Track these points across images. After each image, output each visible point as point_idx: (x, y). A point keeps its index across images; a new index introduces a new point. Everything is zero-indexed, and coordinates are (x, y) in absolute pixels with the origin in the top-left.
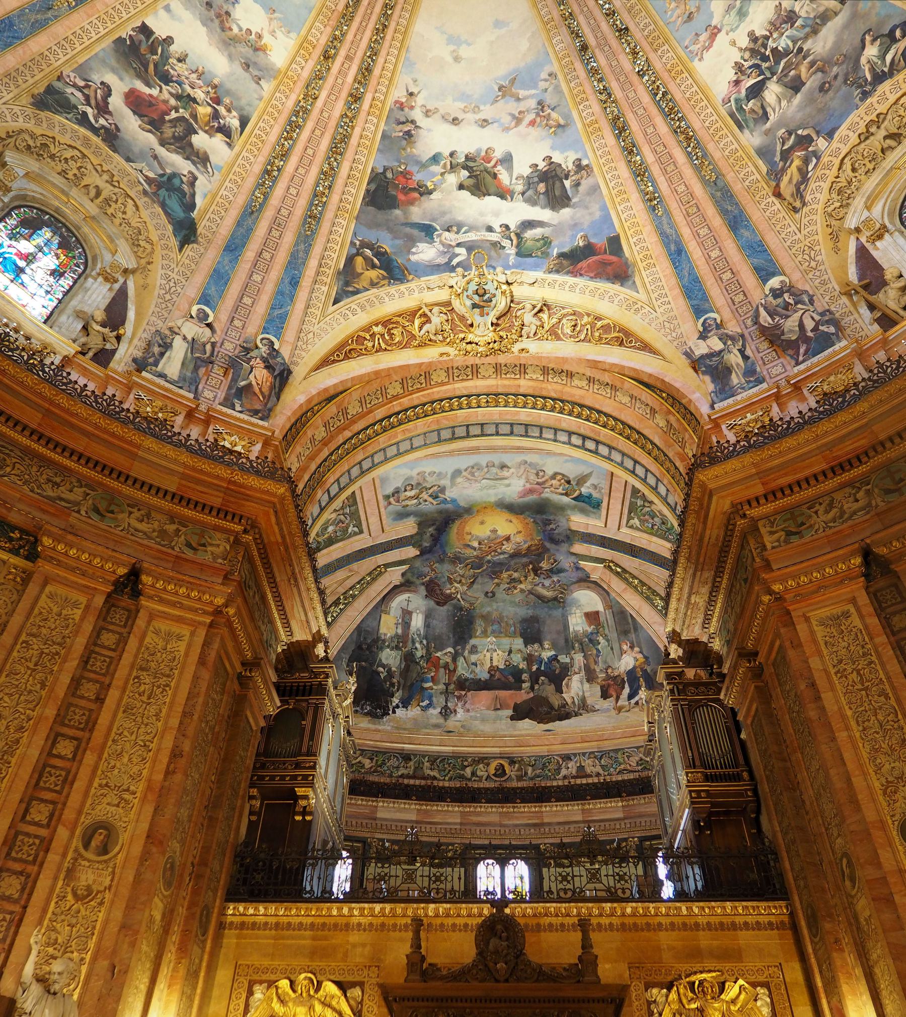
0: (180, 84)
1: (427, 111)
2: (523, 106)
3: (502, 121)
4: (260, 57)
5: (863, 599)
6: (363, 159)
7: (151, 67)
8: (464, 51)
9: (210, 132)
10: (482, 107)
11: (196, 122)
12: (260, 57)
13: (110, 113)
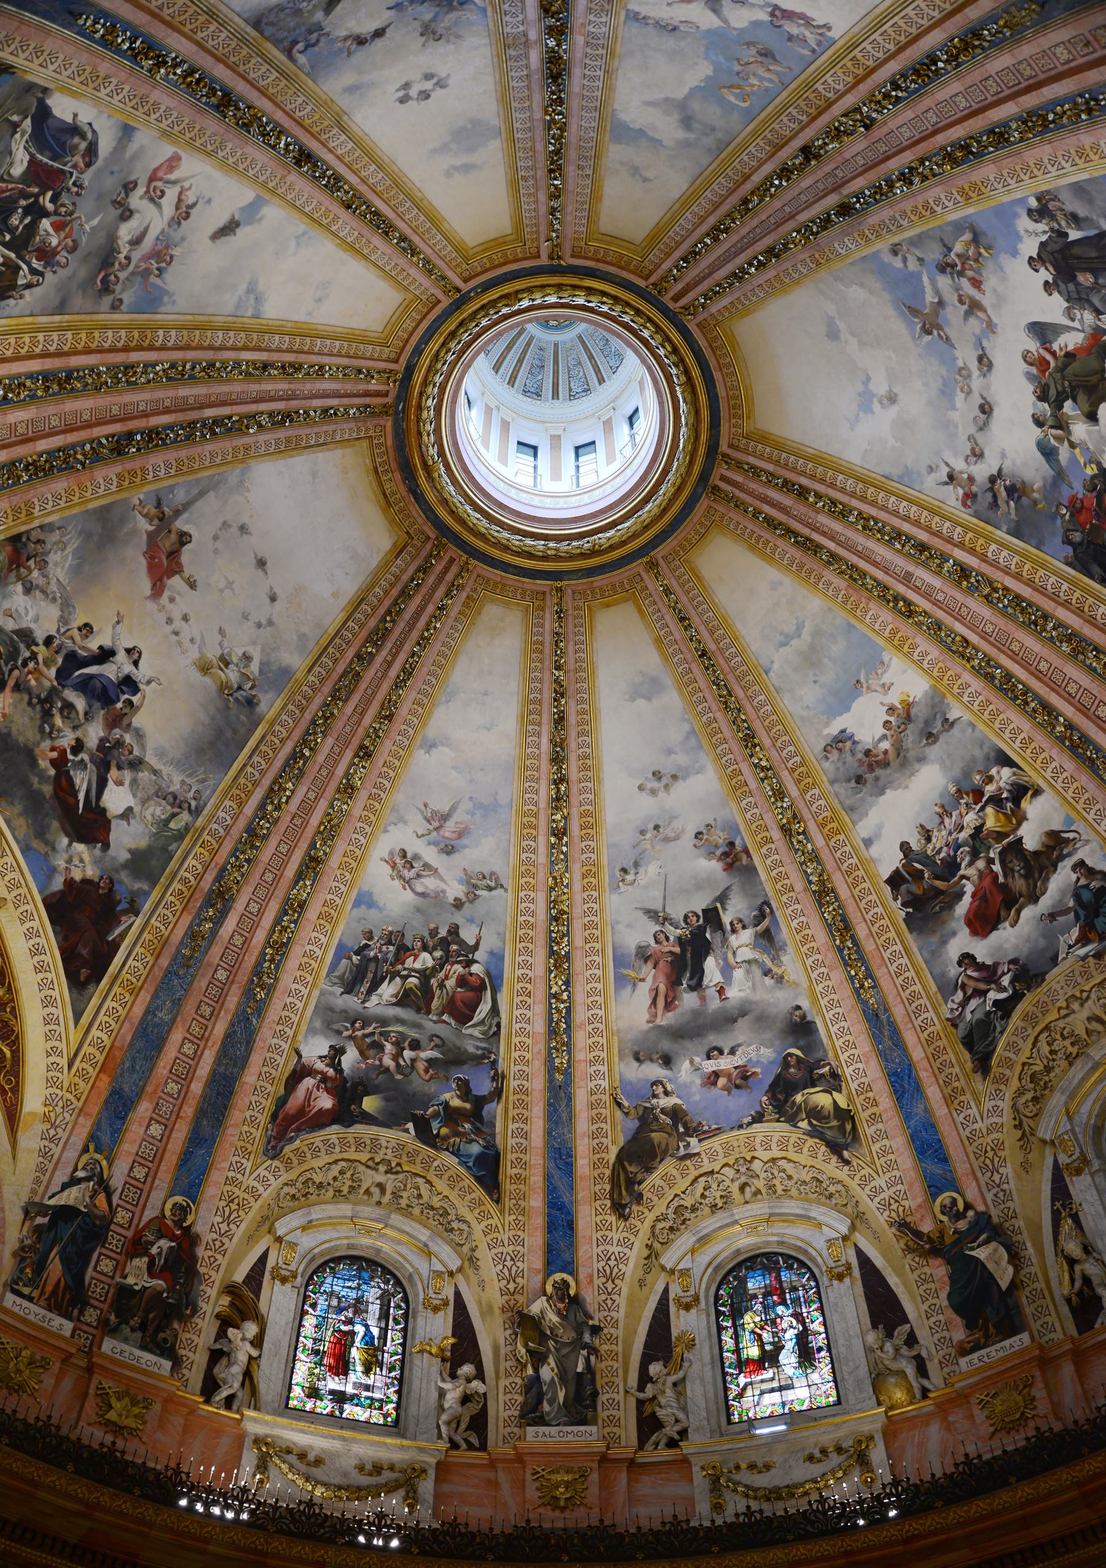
0: (959, 847)
1: (975, 455)
2: (951, 297)
3: (978, 332)
4: (920, 712)
6: (1053, 579)
7: (938, 884)
8: (880, 387)
9: (1022, 819)
10: (960, 363)
11: (1006, 835)
12: (920, 712)
13: (996, 965)
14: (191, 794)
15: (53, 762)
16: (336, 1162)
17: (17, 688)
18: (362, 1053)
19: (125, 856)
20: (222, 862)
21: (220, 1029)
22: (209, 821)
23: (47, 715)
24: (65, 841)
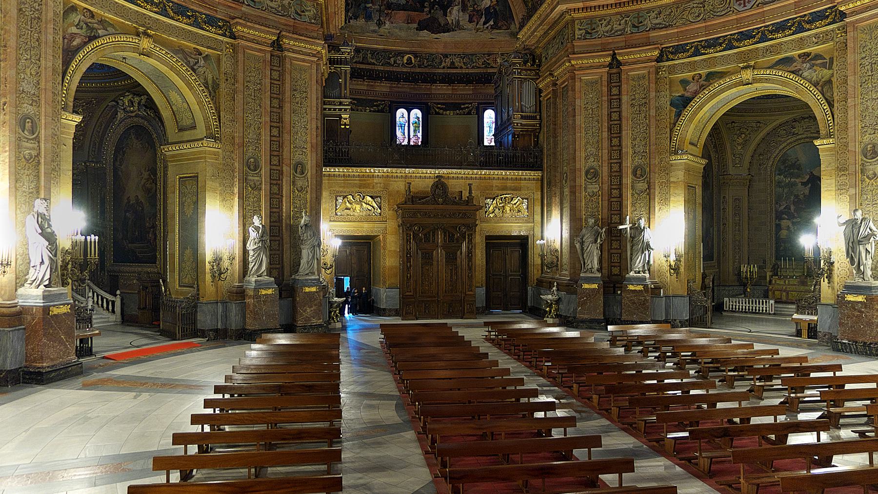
5: (605, 78)
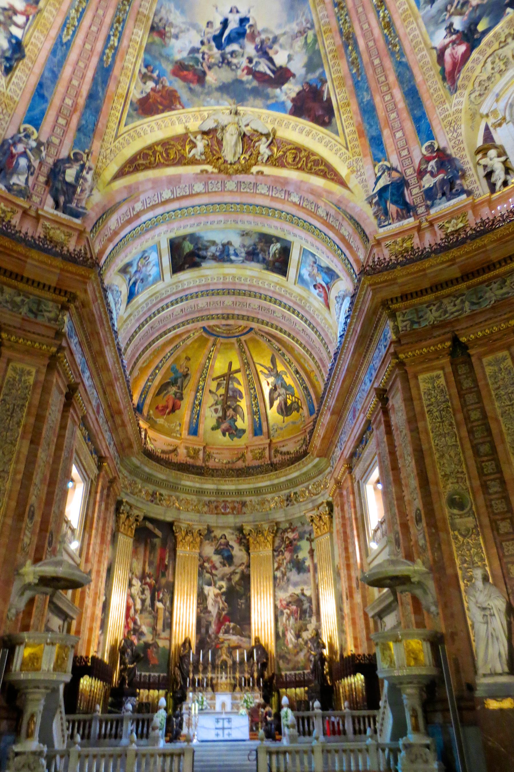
14: (304, 23)
15: (248, 74)
16: (485, 62)
17: (210, 68)
18: (461, 14)
19: (303, 71)
20: (337, 28)
21: (392, 78)
22: (319, 23)
23: (229, 64)
24: (278, 91)
